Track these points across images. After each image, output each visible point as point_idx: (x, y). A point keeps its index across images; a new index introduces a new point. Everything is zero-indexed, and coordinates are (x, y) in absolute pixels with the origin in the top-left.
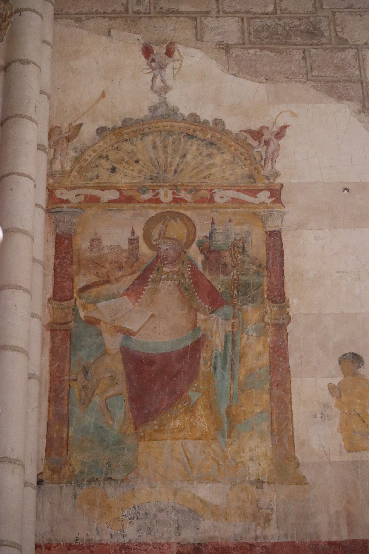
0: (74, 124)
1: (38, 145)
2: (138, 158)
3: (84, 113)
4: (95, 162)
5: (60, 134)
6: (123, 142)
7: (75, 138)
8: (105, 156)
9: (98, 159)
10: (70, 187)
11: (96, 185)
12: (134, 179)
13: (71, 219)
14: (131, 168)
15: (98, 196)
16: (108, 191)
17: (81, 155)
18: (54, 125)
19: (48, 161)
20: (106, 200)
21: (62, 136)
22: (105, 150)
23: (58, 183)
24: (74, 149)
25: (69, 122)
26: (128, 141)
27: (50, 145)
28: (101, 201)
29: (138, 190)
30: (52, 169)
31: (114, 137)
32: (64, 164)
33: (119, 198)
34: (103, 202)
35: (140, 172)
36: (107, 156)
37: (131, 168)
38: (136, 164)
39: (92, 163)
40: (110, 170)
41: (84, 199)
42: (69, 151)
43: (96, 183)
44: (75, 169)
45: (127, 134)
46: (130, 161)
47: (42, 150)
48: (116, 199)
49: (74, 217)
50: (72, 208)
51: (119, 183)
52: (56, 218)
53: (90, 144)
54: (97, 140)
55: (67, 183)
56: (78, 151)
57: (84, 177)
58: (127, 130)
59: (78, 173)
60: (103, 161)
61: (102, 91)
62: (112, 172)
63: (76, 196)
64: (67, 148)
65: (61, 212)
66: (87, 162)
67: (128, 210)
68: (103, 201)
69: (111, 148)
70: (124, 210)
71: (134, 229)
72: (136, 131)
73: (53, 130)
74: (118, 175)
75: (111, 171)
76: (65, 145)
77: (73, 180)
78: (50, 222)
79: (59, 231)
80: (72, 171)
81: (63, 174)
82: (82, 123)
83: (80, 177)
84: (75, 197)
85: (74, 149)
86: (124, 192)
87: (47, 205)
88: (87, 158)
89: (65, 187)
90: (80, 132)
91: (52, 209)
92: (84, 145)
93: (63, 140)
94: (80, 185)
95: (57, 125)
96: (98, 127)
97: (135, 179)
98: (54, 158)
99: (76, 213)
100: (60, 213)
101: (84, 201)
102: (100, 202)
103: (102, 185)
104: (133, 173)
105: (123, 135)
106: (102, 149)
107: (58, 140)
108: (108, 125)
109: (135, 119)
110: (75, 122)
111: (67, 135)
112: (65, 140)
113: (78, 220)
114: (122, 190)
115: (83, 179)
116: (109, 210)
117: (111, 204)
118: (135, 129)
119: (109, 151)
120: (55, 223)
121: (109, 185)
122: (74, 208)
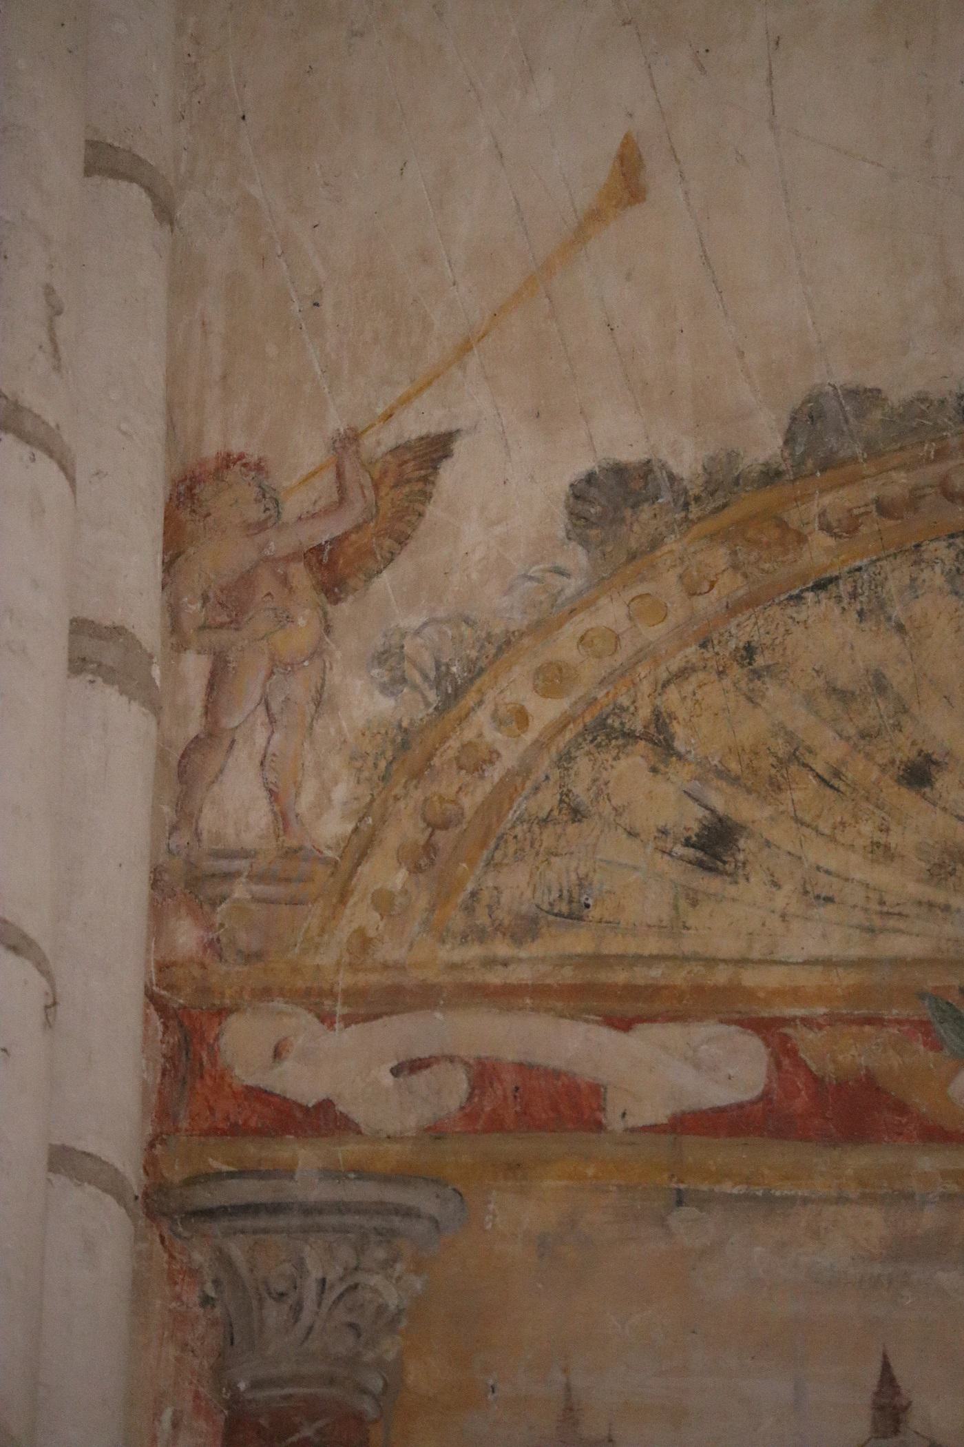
0: (380, 441)
1: (79, 627)
2: (928, 749)
3: (465, 348)
4: (556, 774)
5: (261, 526)
6: (799, 598)
7: (390, 559)
8: (639, 728)
9: (587, 747)
10: (351, 995)
11: (568, 975)
12: (901, 932)
13: (360, 1277)
14: (867, 828)
15: (586, 1072)
16: (672, 1033)
17: (441, 710)
18: (212, 447)
19: (162, 757)
20: (655, 1112)
21: (278, 544)
22: (642, 671)
23: (250, 957)
24: (381, 658)
25: (336, 423)
26: (844, 588)
27: (173, 612)
28: (613, 1121)
29: (924, 1026)
30: (197, 834)
31: (719, 557)
32: (298, 786)
33: (765, 1096)
34: (633, 1130)
35: (941, 866)
36: (660, 721)
37: (867, 828)
38: (907, 798)
39: (537, 789)
40: (688, 843)
41: (470, 1097)
42: (335, 677)
43: (564, 960)
44: (392, 838)
45: (827, 528)
46: (860, 770)
47: (109, 675)
48: (740, 1106)
49: (381, 1254)
50: (362, 1174)
51: (760, 962)
52: (224, 1260)
53: (519, 621)
54: (572, 585)
55: (326, 959)
56: (418, 678)
57: (469, 909)
58: (827, 500)
59: (416, 869)
60: (623, 764)
61: (613, 144)
62: (700, 864)
63: (395, 1072)
64: (317, 652)
65: (275, 1209)
66: (495, 774)
67: (841, 1200)
68: (632, 1122)
69: (692, 651)
70: (805, 1201)
71: (897, 1371)
72: (914, 499)
73: (205, 491)
74: (756, 887)
75: (690, 852)
76: (305, 621)
77: (371, 933)
78: (178, 1298)
79: (256, 1385)
80: (363, 855)
81: (288, 880)
82: (443, 429)
83: (432, 908)
84: (388, 1080)
85: (381, 658)
86: (809, 1043)
87: (152, 1145)
88: (493, 736)
89: (308, 992)
90: (433, 511)
91: (190, 1182)
92: (467, 621)
93: (285, 581)
94: (431, 976)
95: (237, 444)
96: (584, 465)
97: (901, 925)
98: (210, 735)
99: (397, 1222)
100: (263, 1222)
101: (470, 1114)
102: (599, 1126)
103: (621, 977)
104: (883, 876)
105: (801, 539)
106: (620, 658)
107: (246, 580)
108: (664, 454)
109: (897, 396)
110: (388, 416)
111: (325, 531)
112: (300, 576)
113: (418, 1284)
114: (785, 1021)
115: (458, 921)
116: (680, 1199)
117: (695, 1149)
118: (899, 483)
119: (683, 673)
120: (218, 1311)
121: (680, 977)
122: (387, 1179)
